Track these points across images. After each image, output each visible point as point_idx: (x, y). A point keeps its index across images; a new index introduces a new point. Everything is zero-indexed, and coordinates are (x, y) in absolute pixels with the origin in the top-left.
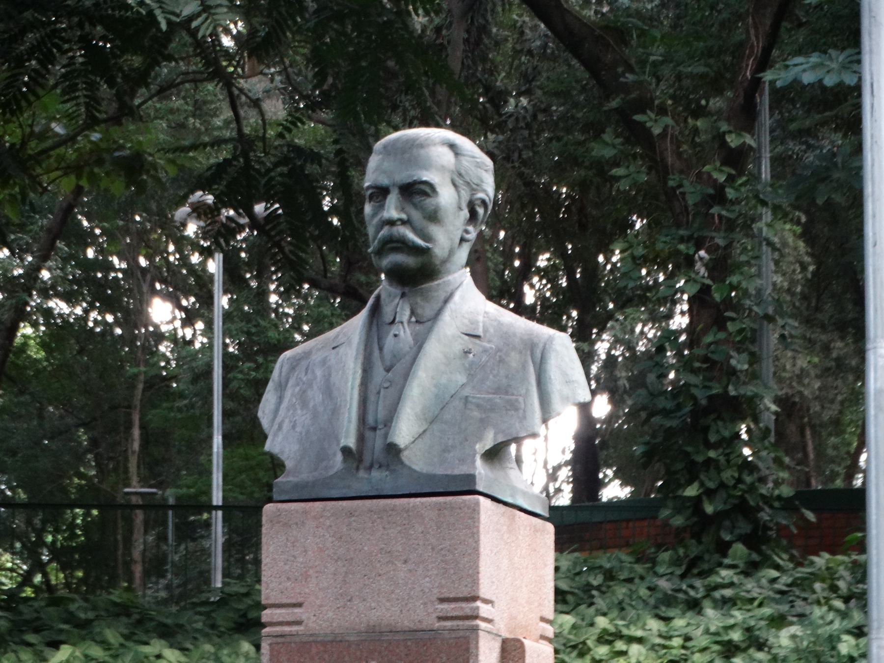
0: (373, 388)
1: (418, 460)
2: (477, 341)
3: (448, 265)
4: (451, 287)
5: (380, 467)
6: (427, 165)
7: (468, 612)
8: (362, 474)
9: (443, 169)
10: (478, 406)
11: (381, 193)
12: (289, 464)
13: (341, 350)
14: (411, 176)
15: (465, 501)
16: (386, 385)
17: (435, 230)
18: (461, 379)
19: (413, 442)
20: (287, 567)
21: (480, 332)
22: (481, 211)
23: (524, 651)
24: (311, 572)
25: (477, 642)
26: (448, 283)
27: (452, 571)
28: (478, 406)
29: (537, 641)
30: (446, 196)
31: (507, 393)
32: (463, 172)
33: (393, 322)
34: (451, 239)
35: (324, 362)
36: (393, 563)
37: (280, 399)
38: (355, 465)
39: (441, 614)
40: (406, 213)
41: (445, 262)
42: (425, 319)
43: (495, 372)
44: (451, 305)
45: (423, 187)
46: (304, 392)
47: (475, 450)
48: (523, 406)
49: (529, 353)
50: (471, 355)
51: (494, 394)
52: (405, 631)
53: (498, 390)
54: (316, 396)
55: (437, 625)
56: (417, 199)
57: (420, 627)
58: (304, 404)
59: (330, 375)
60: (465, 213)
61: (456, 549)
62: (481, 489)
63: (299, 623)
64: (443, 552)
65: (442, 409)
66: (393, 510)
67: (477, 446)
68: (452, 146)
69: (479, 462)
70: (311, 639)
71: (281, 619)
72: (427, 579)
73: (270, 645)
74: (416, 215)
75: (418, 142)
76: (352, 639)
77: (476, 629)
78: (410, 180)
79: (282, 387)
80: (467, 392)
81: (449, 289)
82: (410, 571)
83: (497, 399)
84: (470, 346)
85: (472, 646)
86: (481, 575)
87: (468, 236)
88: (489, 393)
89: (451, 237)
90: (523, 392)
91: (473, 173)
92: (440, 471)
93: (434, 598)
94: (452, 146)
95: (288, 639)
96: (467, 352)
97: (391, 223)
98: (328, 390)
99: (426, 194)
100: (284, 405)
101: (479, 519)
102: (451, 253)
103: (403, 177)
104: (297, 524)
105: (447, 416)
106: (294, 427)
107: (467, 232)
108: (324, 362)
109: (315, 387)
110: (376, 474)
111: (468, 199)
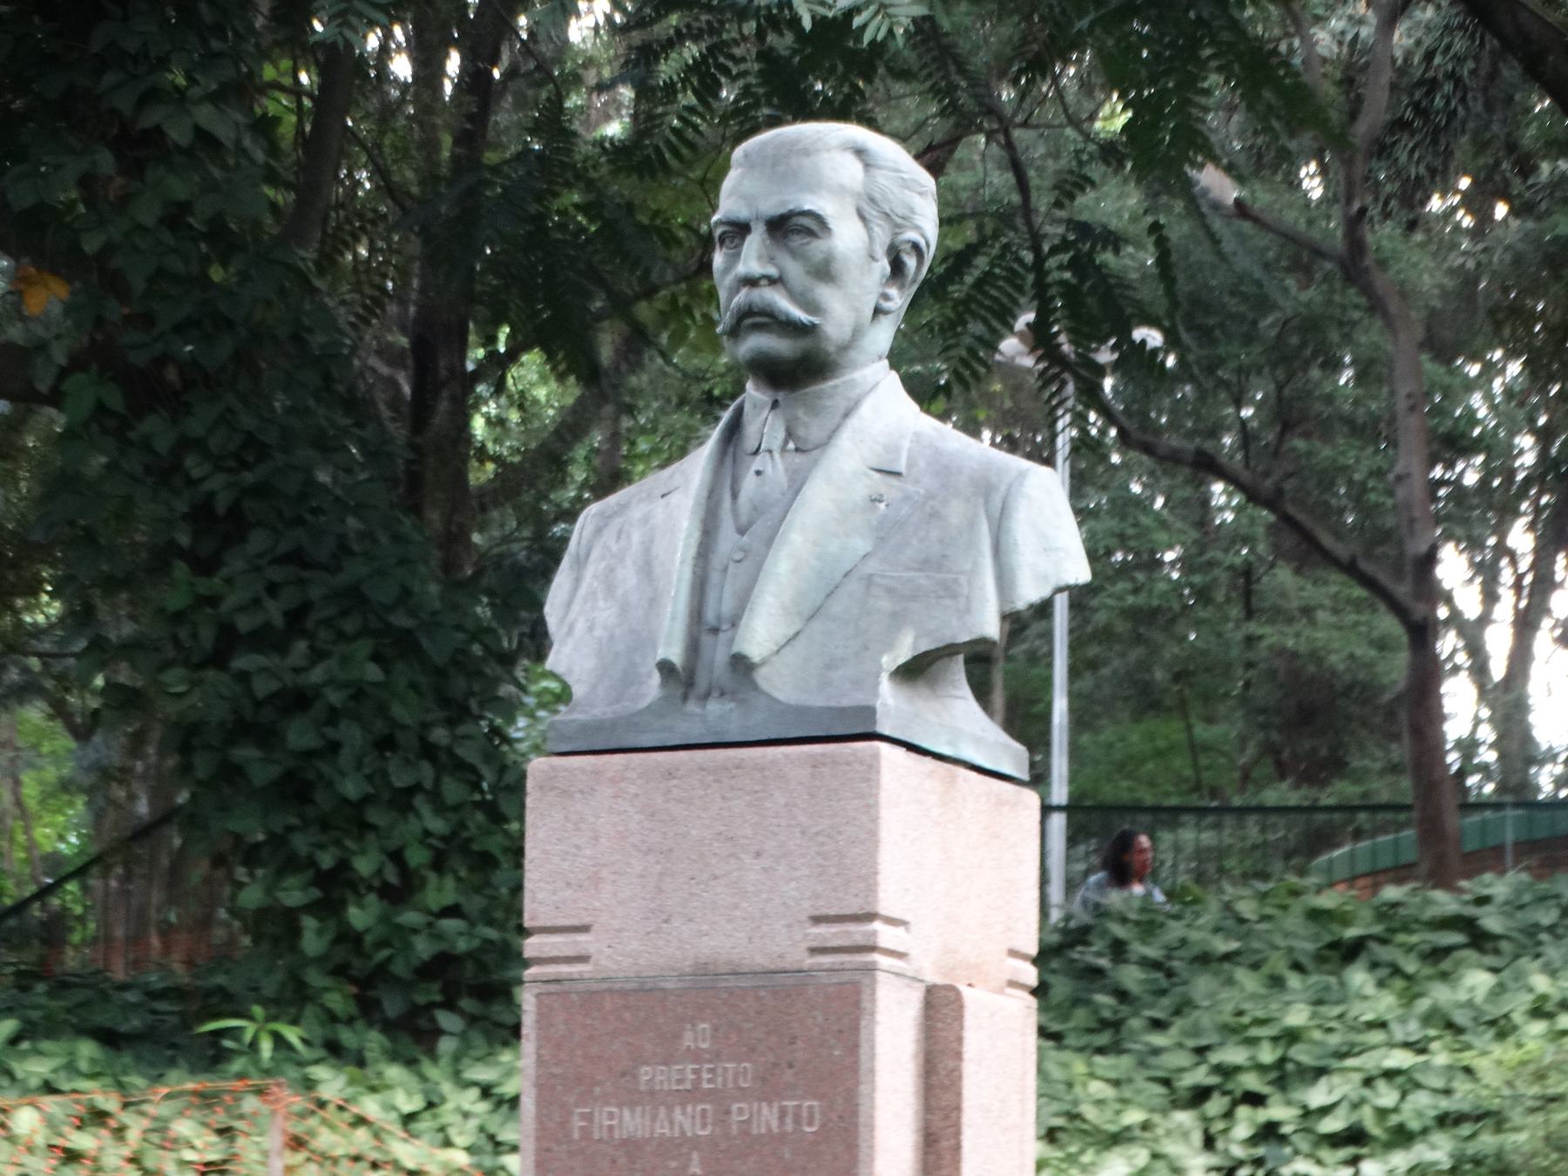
0: (717, 561)
1: (783, 683)
2: (893, 481)
3: (852, 354)
4: (858, 391)
5: (722, 694)
6: (814, 185)
7: (859, 940)
8: (692, 707)
9: (841, 190)
10: (890, 591)
11: (740, 229)
12: (578, 691)
13: (674, 498)
14: (784, 203)
15: (854, 753)
16: (738, 556)
17: (826, 294)
18: (862, 545)
19: (778, 651)
20: (566, 865)
21: (901, 467)
22: (911, 262)
23: (961, 1007)
24: (604, 873)
25: (873, 992)
26: (852, 384)
27: (833, 871)
28: (890, 591)
29: (1000, 991)
30: (847, 237)
31: (939, 569)
32: (878, 196)
33: (756, 452)
34: (856, 310)
35: (646, 520)
36: (738, 858)
37: (577, 581)
38: (680, 691)
39: (814, 944)
40: (776, 265)
41: (844, 348)
42: (810, 446)
43: (922, 534)
44: (853, 422)
45: (806, 221)
46: (612, 570)
47: (881, 666)
48: (965, 591)
49: (981, 500)
50: (882, 506)
51: (920, 570)
52: (755, 973)
53: (925, 564)
54: (628, 576)
55: (810, 961)
56: (797, 241)
57: (780, 965)
58: (610, 588)
59: (652, 541)
60: (884, 265)
61: (840, 833)
62: (887, 732)
63: (582, 959)
64: (821, 839)
65: (828, 596)
66: (738, 767)
67: (885, 659)
68: (860, 152)
69: (886, 686)
70: (604, 986)
71: (555, 953)
72: (793, 884)
73: (538, 996)
74: (794, 270)
75: (800, 146)
76: (669, 985)
77: (871, 969)
78: (782, 210)
79: (580, 563)
80: (872, 566)
81: (853, 395)
82: (765, 870)
83: (922, 580)
84: (883, 490)
85: (865, 997)
86: (880, 878)
87: (886, 305)
88: (908, 569)
89: (860, 307)
90: (968, 567)
91: (898, 199)
92: (817, 701)
93: (804, 917)
94: (860, 152)
95: (566, 986)
96: (876, 500)
97: (751, 282)
98: (647, 568)
99: (811, 233)
100: (583, 591)
101: (878, 781)
102: (857, 333)
103: (772, 206)
104: (582, 792)
105: (836, 607)
106: (591, 629)
107: (886, 297)
108: (646, 520)
109: (629, 562)
110: (714, 707)
111: (887, 241)
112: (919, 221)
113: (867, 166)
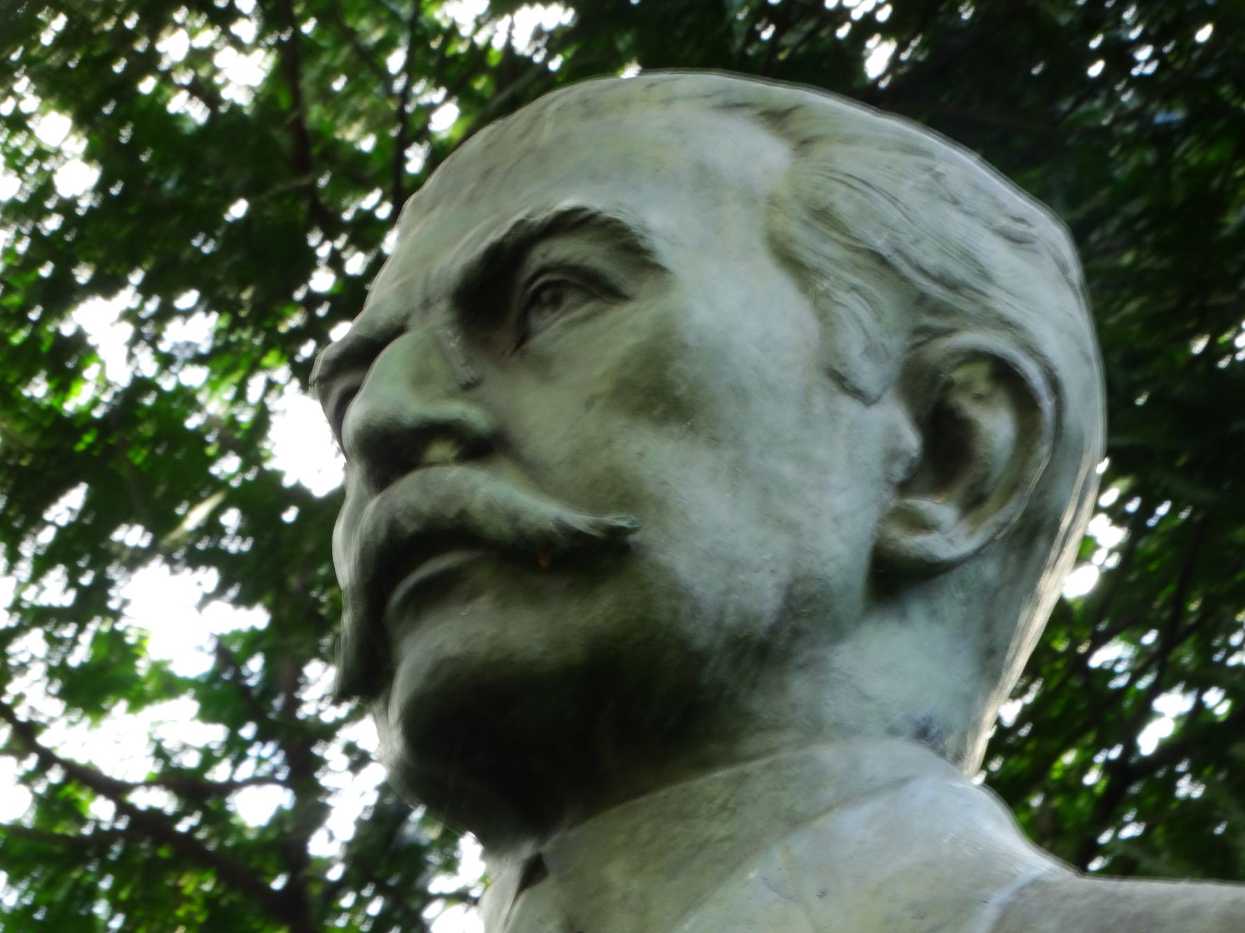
3: (799, 687)
22: (996, 426)
45: (563, 250)
60: (894, 427)
68: (776, 118)
99: (600, 289)
111: (896, 344)
112: (1002, 304)
113: (804, 144)
